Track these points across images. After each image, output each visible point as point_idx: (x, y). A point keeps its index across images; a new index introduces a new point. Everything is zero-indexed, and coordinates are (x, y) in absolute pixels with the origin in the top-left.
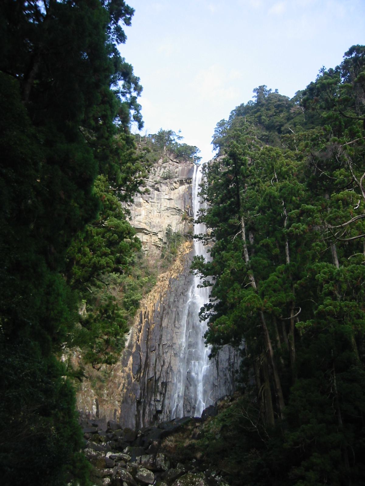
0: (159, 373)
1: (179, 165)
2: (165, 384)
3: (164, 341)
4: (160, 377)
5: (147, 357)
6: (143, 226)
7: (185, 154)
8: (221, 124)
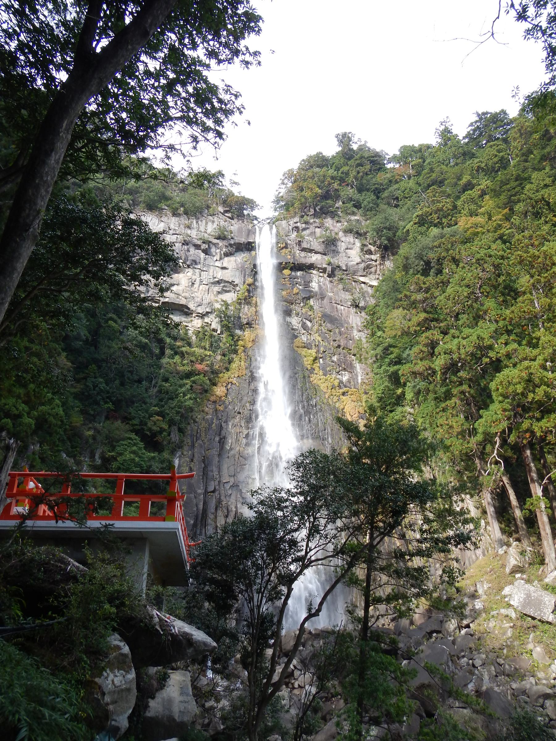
1: (233, 222)
6: (183, 302)
8: (290, 174)
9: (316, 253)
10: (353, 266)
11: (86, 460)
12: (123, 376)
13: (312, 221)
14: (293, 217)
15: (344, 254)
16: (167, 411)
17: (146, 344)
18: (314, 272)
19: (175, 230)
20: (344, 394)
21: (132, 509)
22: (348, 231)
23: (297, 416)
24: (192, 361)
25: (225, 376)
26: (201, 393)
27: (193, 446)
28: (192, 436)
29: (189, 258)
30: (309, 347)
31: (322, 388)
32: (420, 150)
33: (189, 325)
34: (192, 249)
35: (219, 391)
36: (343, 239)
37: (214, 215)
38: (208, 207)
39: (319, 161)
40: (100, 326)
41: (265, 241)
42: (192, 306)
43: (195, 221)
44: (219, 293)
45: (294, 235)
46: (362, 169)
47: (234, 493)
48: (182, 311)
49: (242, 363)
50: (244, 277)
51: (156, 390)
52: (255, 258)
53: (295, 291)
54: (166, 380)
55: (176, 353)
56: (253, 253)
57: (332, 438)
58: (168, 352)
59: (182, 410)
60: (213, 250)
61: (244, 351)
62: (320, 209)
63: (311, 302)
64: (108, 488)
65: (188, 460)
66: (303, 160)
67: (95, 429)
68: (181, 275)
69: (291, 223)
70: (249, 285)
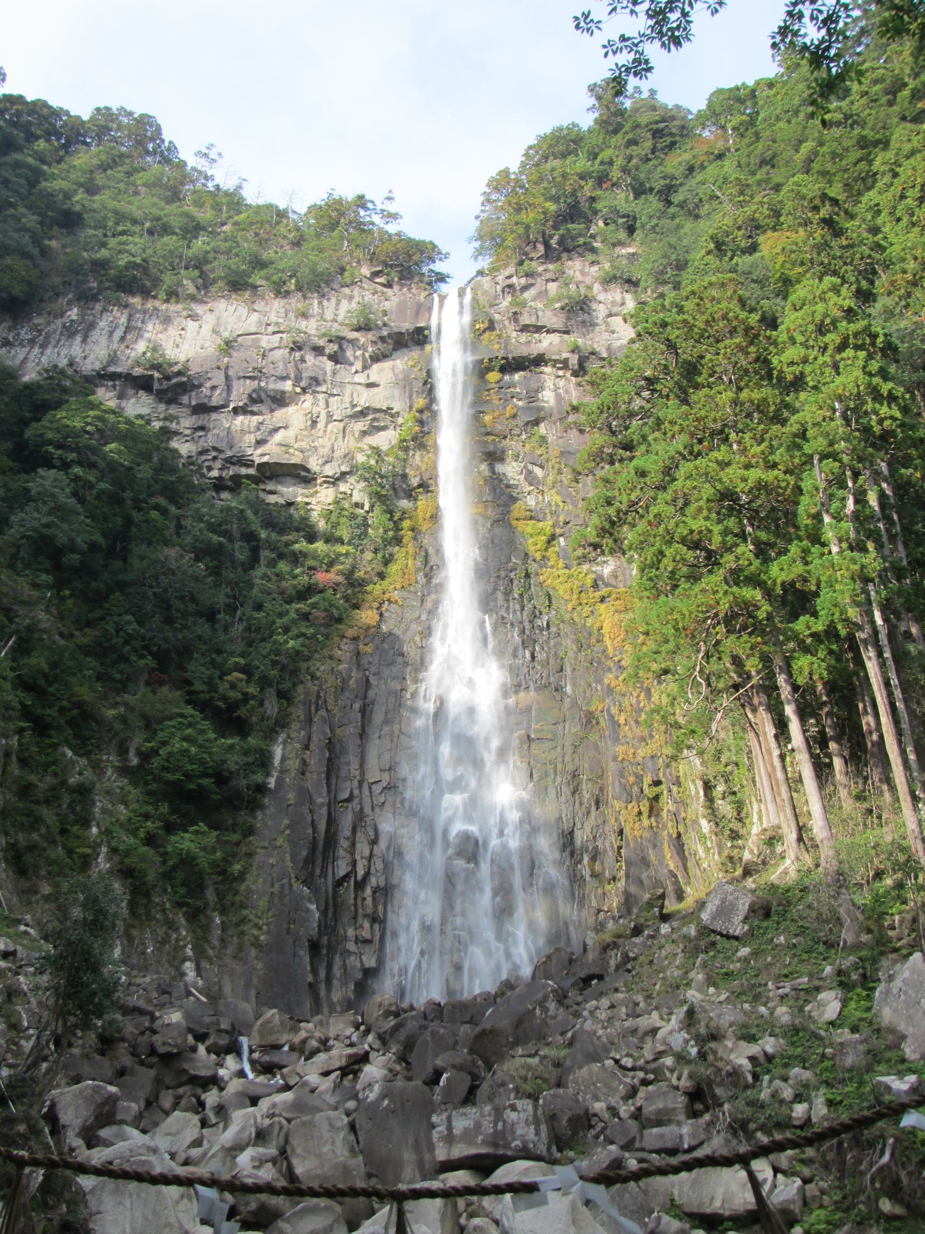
0: (365, 862)
2: (385, 892)
3: (373, 775)
4: (367, 874)
5: (331, 821)
6: (296, 459)
7: (408, 263)
8: (501, 181)
9: (548, 332)
10: (621, 348)
11: (110, 758)
12: (169, 607)
13: (540, 269)
14: (506, 266)
15: (603, 327)
16: (256, 663)
17: (220, 544)
18: (548, 369)
19: (277, 324)
20: (602, 600)
21: (187, 835)
22: (608, 281)
23: (510, 650)
24: (310, 568)
25: (376, 589)
26: (327, 625)
27: (309, 721)
28: (307, 703)
29: (305, 375)
30: (541, 516)
31: (561, 592)
32: (753, 94)
33: (313, 501)
34: (310, 358)
35: (367, 616)
36: (601, 297)
37: (353, 283)
38: (342, 270)
39: (562, 143)
40: (129, 522)
41: (450, 321)
42: (314, 464)
43: (316, 302)
44: (364, 433)
45: (506, 302)
46: (635, 150)
47: (390, 799)
48: (298, 476)
49: (410, 562)
50: (410, 397)
51: (241, 627)
52: (429, 360)
53: (509, 412)
54: (259, 607)
55: (281, 556)
56: (428, 348)
57: (574, 685)
58: (265, 554)
59: (283, 659)
60: (349, 354)
61: (415, 538)
62: (560, 243)
63: (542, 429)
64: (149, 803)
65: (297, 745)
66: (530, 148)
67: (126, 705)
68: (291, 409)
69: (500, 278)
70: (421, 411)
